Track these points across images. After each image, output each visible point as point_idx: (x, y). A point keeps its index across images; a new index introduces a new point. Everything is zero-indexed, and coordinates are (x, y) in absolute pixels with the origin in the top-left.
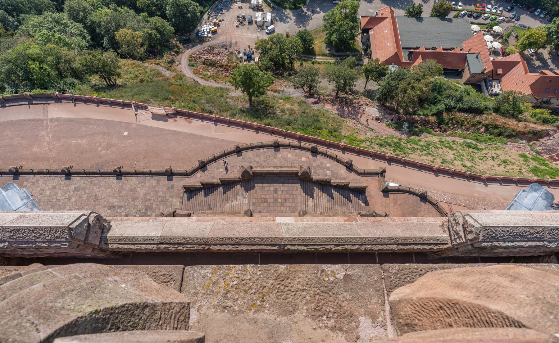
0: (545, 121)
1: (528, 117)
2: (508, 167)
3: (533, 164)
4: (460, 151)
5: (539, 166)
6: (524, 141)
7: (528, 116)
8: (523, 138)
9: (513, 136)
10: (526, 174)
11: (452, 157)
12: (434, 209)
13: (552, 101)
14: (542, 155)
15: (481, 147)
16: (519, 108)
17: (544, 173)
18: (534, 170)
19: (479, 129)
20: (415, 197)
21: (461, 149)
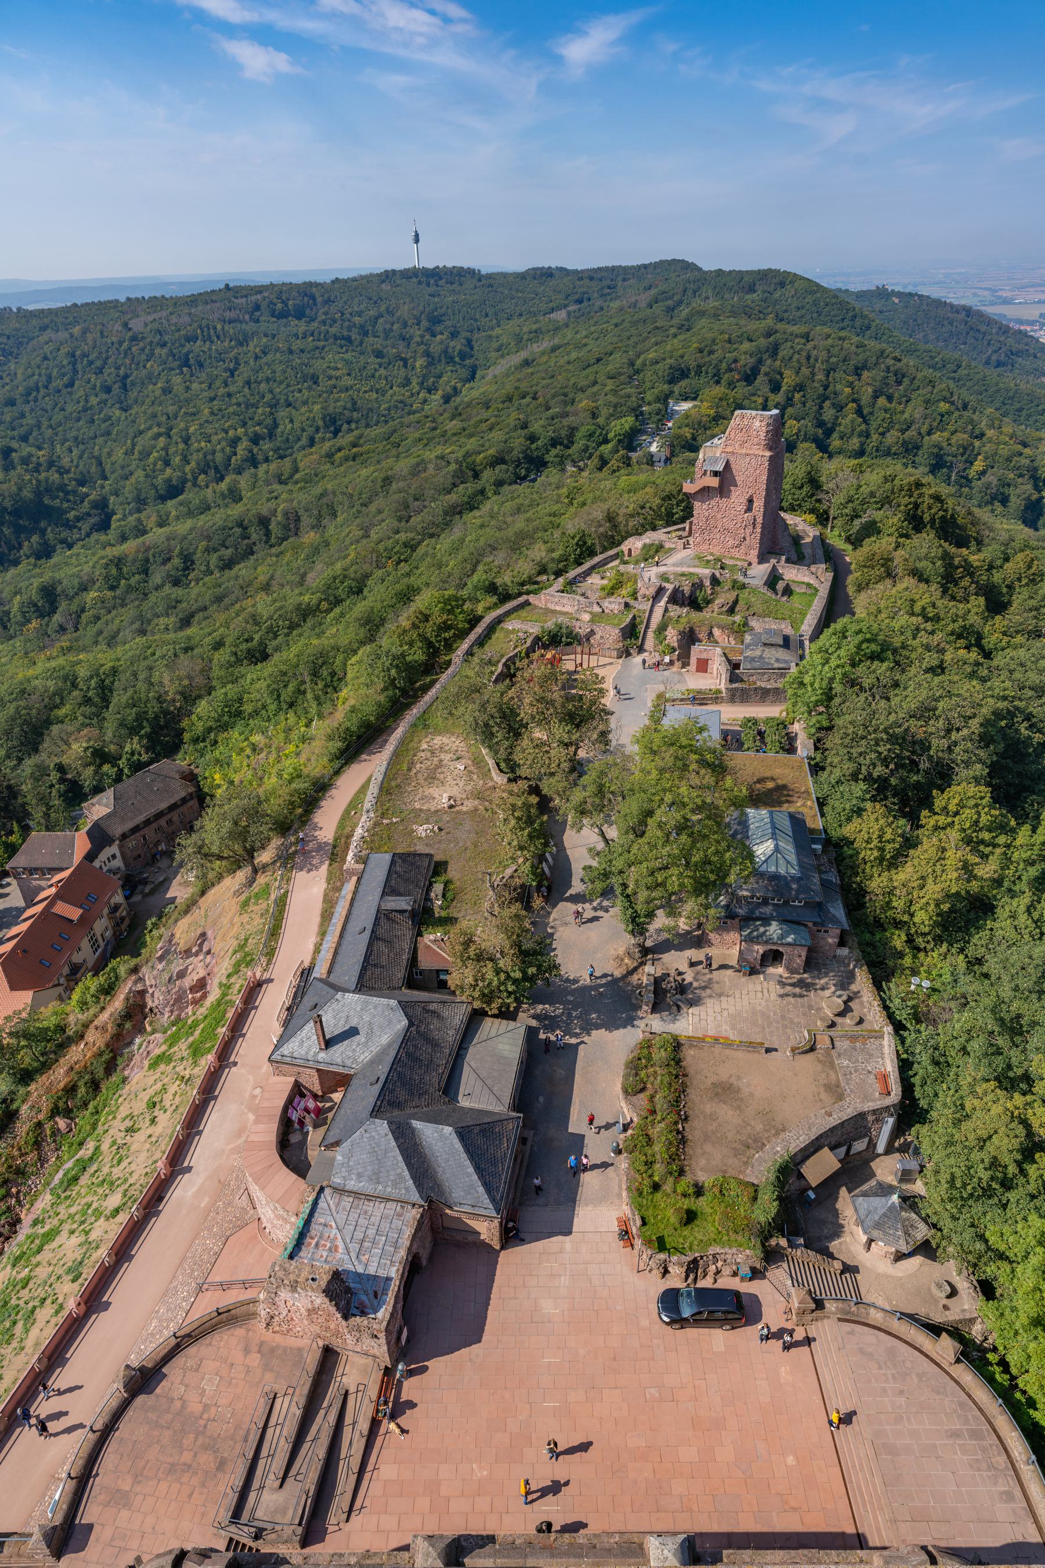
0: (108, 990)
1: (83, 1017)
2: (167, 1103)
3: (182, 1048)
4: (73, 1210)
5: (191, 1039)
6: (138, 1041)
7: (80, 1016)
9: (114, 1059)
10: (197, 1070)
11: (75, 1240)
12: (192, 1350)
13: (77, 958)
14: (183, 1015)
15: (90, 1153)
16: (48, 1029)
17: (209, 1034)
18: (196, 1051)
19: (56, 1132)
20: (130, 1413)
21: (70, 1206)
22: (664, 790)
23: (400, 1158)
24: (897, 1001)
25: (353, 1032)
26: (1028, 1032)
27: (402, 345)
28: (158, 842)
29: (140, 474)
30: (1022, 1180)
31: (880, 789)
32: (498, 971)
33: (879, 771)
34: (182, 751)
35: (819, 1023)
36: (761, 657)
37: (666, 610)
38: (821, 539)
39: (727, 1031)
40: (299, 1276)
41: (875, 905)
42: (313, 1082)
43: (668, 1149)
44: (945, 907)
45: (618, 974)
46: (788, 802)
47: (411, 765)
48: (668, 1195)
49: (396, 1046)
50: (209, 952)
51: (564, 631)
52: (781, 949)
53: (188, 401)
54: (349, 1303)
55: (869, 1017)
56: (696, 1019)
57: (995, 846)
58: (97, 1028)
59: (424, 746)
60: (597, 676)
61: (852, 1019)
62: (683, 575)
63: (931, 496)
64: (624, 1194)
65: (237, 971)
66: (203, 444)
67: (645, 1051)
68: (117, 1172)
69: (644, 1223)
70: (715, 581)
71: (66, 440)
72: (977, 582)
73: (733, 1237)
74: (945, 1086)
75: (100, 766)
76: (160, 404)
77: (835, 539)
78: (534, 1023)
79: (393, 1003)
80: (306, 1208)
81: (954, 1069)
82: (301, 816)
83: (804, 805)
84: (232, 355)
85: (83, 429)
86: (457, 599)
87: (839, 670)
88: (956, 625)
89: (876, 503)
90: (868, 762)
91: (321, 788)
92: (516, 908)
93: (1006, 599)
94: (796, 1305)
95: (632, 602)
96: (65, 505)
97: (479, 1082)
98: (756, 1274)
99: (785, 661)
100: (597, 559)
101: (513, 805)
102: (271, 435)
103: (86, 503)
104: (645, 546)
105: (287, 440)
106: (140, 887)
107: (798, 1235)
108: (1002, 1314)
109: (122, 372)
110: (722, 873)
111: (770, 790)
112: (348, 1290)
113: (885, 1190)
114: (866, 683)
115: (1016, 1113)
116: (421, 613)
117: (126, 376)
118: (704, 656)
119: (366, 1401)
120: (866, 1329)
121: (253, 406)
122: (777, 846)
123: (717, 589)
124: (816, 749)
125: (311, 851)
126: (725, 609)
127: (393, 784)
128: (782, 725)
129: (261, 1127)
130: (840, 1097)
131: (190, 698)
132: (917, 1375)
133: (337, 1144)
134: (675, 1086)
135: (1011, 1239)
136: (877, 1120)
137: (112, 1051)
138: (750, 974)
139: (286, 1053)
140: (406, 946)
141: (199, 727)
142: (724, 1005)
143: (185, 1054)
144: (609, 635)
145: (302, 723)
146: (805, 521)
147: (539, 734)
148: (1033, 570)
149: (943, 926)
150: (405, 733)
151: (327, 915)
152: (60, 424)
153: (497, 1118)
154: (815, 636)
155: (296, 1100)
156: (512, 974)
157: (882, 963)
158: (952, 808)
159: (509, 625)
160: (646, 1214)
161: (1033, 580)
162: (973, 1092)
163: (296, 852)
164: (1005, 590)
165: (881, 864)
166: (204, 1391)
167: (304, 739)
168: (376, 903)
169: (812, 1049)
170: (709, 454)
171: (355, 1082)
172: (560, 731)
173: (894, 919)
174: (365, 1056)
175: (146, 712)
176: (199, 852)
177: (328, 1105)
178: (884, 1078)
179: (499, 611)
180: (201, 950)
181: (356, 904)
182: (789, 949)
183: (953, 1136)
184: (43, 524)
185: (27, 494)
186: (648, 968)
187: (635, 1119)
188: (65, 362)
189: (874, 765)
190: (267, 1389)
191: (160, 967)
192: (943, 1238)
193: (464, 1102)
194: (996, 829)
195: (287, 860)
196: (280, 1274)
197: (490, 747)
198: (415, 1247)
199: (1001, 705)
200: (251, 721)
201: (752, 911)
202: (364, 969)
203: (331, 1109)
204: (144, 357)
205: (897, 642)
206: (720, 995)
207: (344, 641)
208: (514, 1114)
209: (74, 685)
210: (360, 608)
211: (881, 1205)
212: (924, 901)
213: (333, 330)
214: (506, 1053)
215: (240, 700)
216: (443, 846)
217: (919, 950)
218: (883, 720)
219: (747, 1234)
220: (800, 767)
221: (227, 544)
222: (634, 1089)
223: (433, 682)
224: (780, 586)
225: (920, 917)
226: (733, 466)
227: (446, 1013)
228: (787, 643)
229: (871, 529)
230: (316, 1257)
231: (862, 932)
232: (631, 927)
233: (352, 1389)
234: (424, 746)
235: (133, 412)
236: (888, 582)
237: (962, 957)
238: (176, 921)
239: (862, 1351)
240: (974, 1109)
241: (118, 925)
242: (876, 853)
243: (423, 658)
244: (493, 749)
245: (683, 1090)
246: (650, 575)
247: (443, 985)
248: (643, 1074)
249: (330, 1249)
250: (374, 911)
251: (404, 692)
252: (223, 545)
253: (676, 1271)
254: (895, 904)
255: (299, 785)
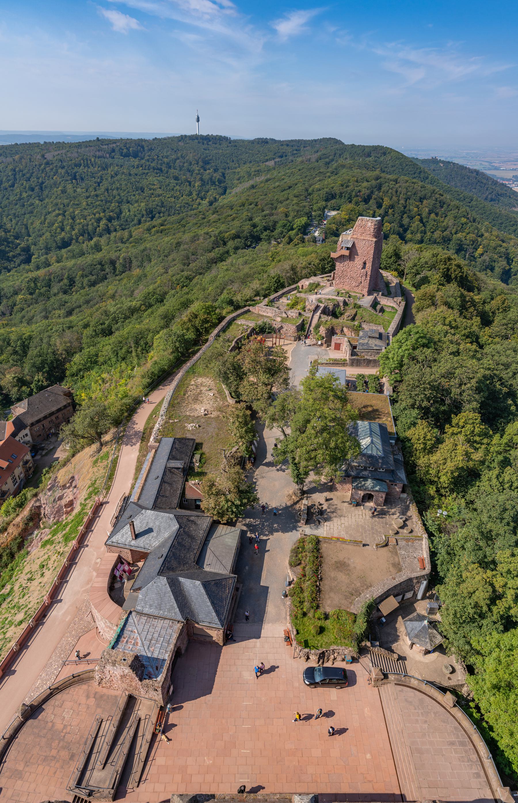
0: (21, 505)
2: (50, 566)
3: (59, 537)
5: (64, 532)
6: (36, 532)
7: (5, 519)
8: (31, 532)
9: (23, 541)
10: (67, 549)
12: (58, 696)
13: (5, 488)
14: (60, 519)
15: (8, 591)
17: (74, 530)
18: (67, 539)
20: (24, 729)
22: (316, 410)
23: (172, 597)
24: (430, 522)
25: (150, 531)
26: (495, 539)
27: (188, 174)
28: (50, 429)
29: (48, 234)
30: (490, 614)
31: (425, 413)
32: (227, 501)
33: (425, 404)
34: (65, 381)
35: (390, 532)
36: (367, 343)
37: (320, 317)
38: (400, 284)
39: (344, 535)
40: (117, 658)
41: (420, 472)
42: (128, 556)
43: (311, 595)
44: (456, 474)
45: (289, 504)
46: (379, 418)
47: (186, 392)
48: (311, 619)
49: (172, 539)
50: (75, 487)
51: (267, 326)
52: (372, 493)
53: (75, 198)
54: (142, 672)
55: (416, 530)
56: (328, 528)
57: (482, 444)
58: (14, 525)
59: (193, 383)
60: (283, 350)
61: (407, 530)
62: (329, 299)
63: (455, 265)
64: (288, 618)
65: (90, 497)
66: (82, 220)
67: (301, 544)
68: (22, 601)
69: (298, 633)
70: (345, 304)
71: (9, 215)
72: (477, 310)
73: (343, 641)
74: (453, 565)
75: (21, 387)
76: (60, 199)
77: (407, 285)
78: (245, 528)
79: (172, 516)
80: (122, 623)
81: (458, 557)
82: (127, 417)
83: (386, 420)
84: (99, 175)
86: (212, 307)
87: (407, 352)
88: (466, 331)
89: (428, 267)
90: (420, 399)
91: (138, 403)
92: (238, 468)
93: (491, 319)
94: (374, 676)
95: (302, 313)
96: (7, 249)
97: (215, 558)
98: (354, 660)
99: (380, 346)
100: (285, 290)
101: (238, 415)
102: (118, 218)
103: (18, 248)
104: (310, 284)
105: (127, 220)
106: (40, 452)
107: (376, 640)
108: (477, 682)
109: (40, 180)
110: (344, 453)
111: (370, 412)
112: (143, 666)
113: (421, 618)
114: (420, 358)
115: (488, 580)
116: (193, 313)
117: (43, 183)
118: (338, 342)
119: (150, 724)
120: (409, 689)
121: (109, 202)
122: (372, 441)
123: (347, 307)
124: (394, 391)
125: (131, 436)
126: (350, 318)
127: (176, 402)
128: (377, 378)
129: (100, 579)
130: (400, 570)
131: (70, 353)
132: (434, 713)
133: (140, 589)
134: (316, 562)
135: (483, 644)
136: (418, 582)
137: (21, 537)
138: (356, 506)
139: (114, 541)
140: (180, 486)
141: (75, 369)
142: (343, 521)
143: (61, 540)
144: (290, 329)
145: (130, 368)
146: (392, 275)
147: (252, 379)
148: (505, 305)
149: (455, 484)
150: (183, 376)
151: (138, 469)
152: (6, 206)
153: (224, 577)
154: (395, 334)
155: (119, 566)
156: (235, 503)
157: (423, 502)
158: (461, 424)
159: (239, 322)
160: (299, 628)
161: (505, 310)
162: (467, 569)
163: (123, 436)
164: (491, 314)
165: (424, 451)
166: (64, 718)
167: (130, 377)
168: (165, 464)
169: (387, 545)
170: (345, 238)
171: (150, 557)
172: (264, 378)
173: (430, 480)
174: (156, 543)
175: (47, 360)
176: (72, 434)
177: (135, 568)
178: (422, 560)
179: (234, 315)
180: (71, 485)
181: (154, 464)
182: (377, 493)
183: (456, 591)
186: (305, 501)
187: (295, 579)
188: (10, 174)
189: (423, 401)
190: (98, 717)
191: (49, 494)
192: (449, 643)
193: (207, 569)
194: (483, 435)
195: (119, 440)
196: (107, 657)
197: (227, 385)
198: (178, 643)
199: (488, 372)
200: (102, 366)
201: (358, 474)
202: (157, 498)
203: (137, 570)
204: (52, 173)
205: (436, 338)
206: (341, 516)
207: (153, 326)
208: (233, 575)
209: (9, 344)
210: (162, 310)
211: (418, 625)
212: (445, 471)
213: (153, 165)
214: (229, 543)
215: (97, 355)
216: (200, 435)
217: (442, 495)
218: (428, 378)
219: (350, 639)
220: (385, 400)
221: (93, 273)
222: (295, 563)
223: (198, 350)
224: (378, 307)
225: (443, 479)
226: (356, 245)
227: (199, 522)
228: (381, 337)
229: (425, 281)
230: (127, 648)
231: (414, 486)
232: (296, 480)
233: (143, 718)
234: (193, 383)
235: (45, 202)
236: (433, 308)
237: (463, 500)
238: (59, 470)
239: (406, 700)
240: (467, 577)
241: (27, 471)
242: (422, 446)
243: (194, 337)
244: (229, 385)
245: (320, 565)
246: (313, 298)
247: (198, 507)
248: (300, 556)
249: (134, 644)
250: (163, 468)
251: (183, 355)
252: (91, 274)
253: (313, 658)
254: (431, 472)
255: (126, 401)
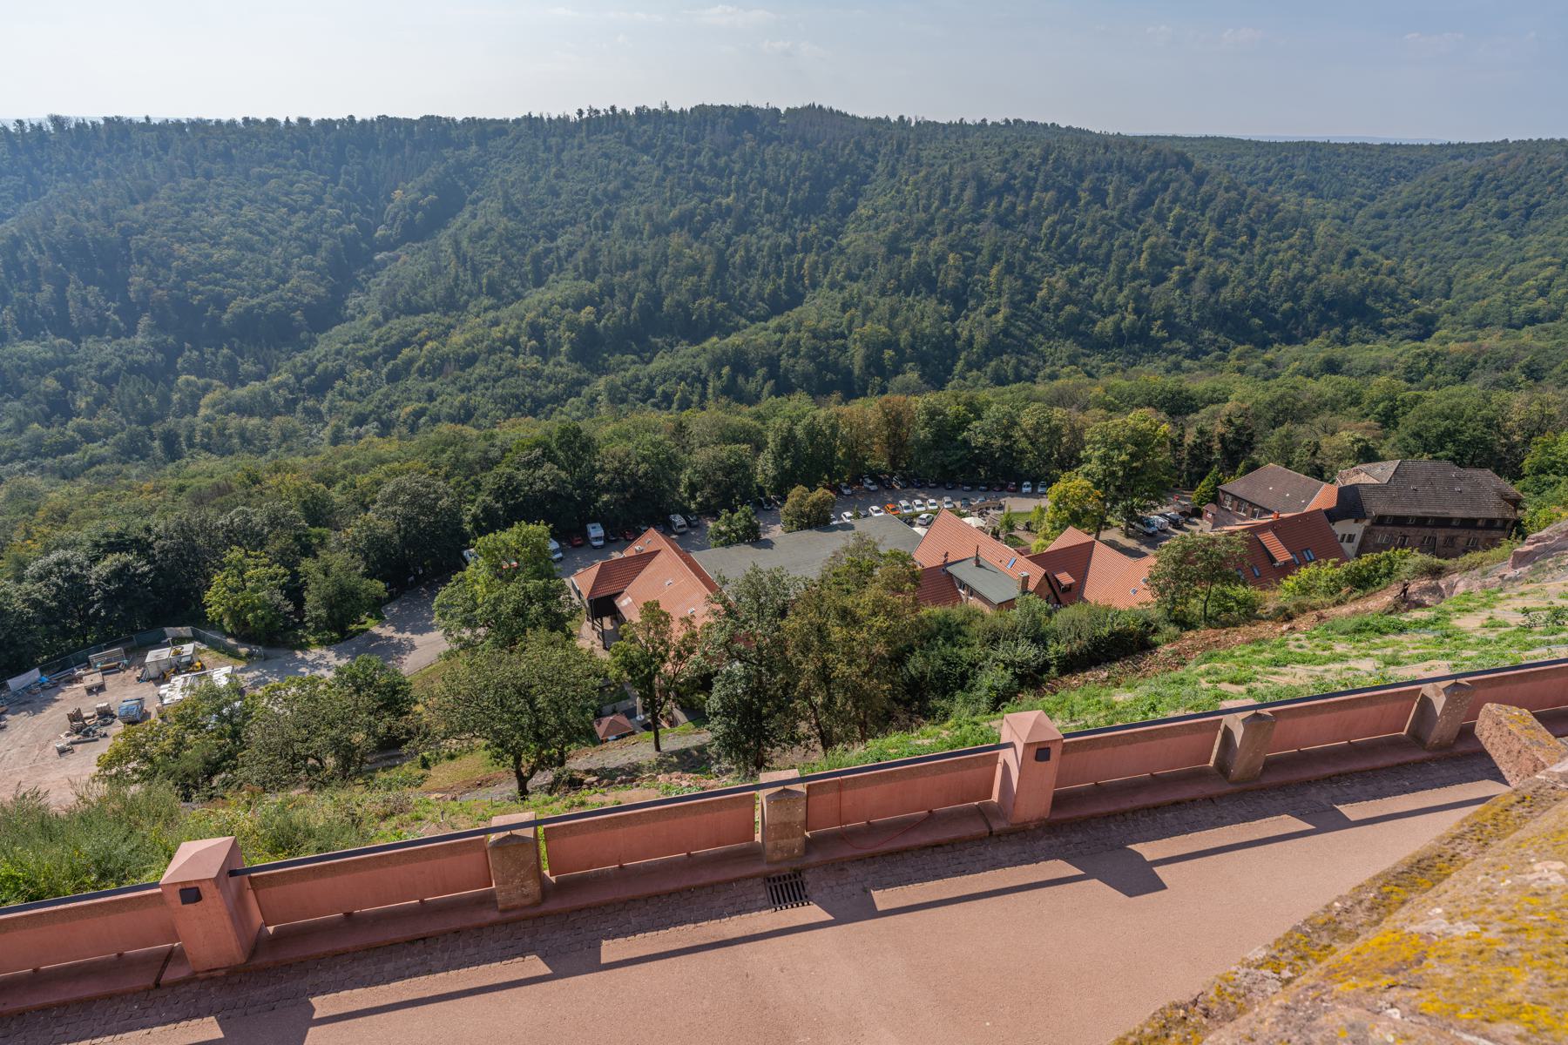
29: (1500, 297)
71: (1421, 255)
85: (1450, 248)
96: (1387, 310)
103: (1411, 315)
109: (1533, 200)
117: (1538, 204)
184: (1352, 321)
185: (1353, 289)
235: (1525, 240)
